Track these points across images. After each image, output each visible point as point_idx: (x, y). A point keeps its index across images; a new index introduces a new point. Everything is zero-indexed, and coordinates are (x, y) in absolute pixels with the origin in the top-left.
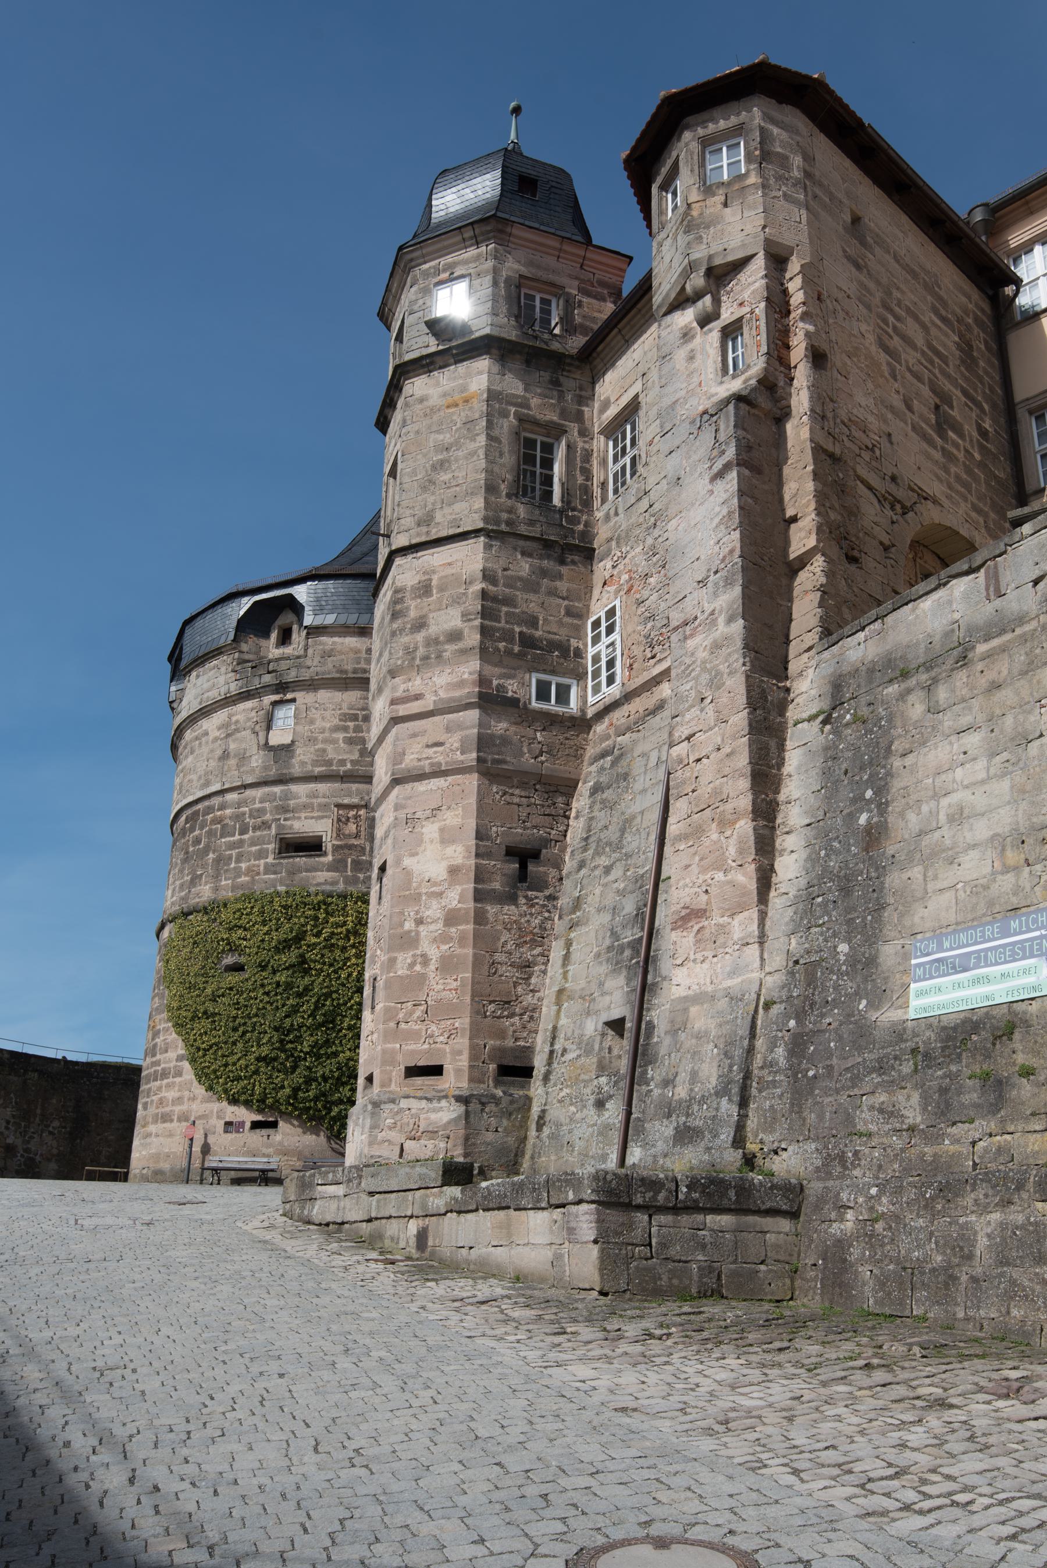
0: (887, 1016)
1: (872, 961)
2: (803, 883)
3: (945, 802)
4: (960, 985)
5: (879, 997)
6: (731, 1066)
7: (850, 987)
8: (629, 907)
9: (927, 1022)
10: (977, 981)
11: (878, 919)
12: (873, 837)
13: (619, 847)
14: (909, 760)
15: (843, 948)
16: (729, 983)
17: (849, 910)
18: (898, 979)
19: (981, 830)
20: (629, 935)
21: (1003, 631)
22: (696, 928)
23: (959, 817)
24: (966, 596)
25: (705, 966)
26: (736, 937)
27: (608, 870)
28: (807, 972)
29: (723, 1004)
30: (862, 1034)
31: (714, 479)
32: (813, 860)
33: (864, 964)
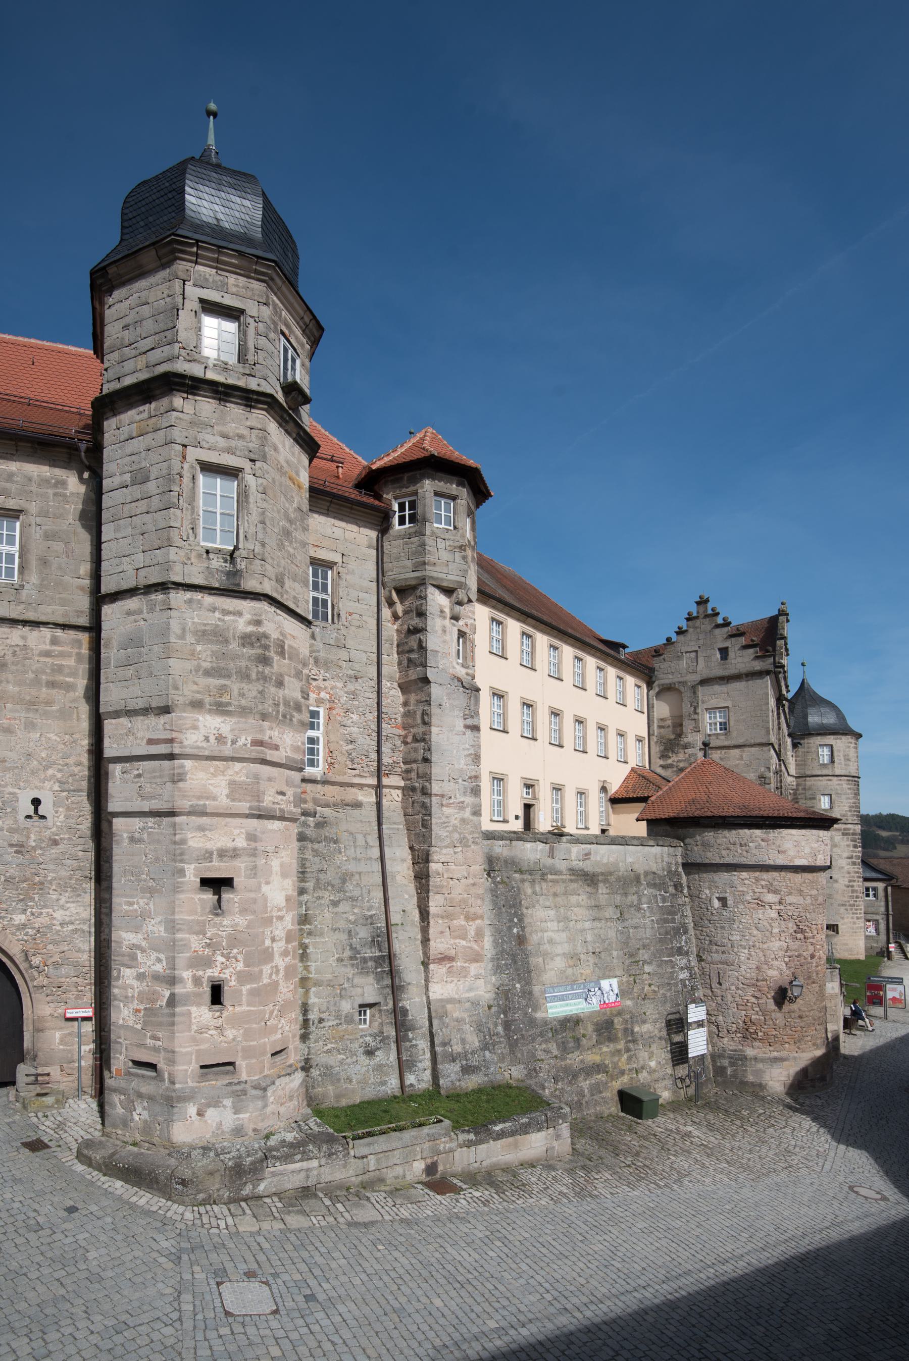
0: (539, 1015)
1: (531, 993)
2: (494, 953)
3: (546, 934)
4: (562, 1006)
5: (536, 1008)
6: (485, 1036)
7: (524, 1003)
8: (364, 933)
9: (555, 1019)
10: (567, 1005)
11: (530, 976)
12: (521, 940)
13: (341, 890)
14: (530, 911)
15: (518, 986)
16: (467, 995)
17: (517, 970)
18: (542, 1001)
19: (559, 950)
20: (368, 953)
21: (555, 874)
22: (448, 965)
23: (551, 941)
24: (541, 851)
25: (453, 985)
26: (472, 974)
27: (335, 904)
28: (504, 994)
29: (468, 1005)
30: (532, 1022)
31: (467, 727)
32: (495, 943)
33: (528, 994)
